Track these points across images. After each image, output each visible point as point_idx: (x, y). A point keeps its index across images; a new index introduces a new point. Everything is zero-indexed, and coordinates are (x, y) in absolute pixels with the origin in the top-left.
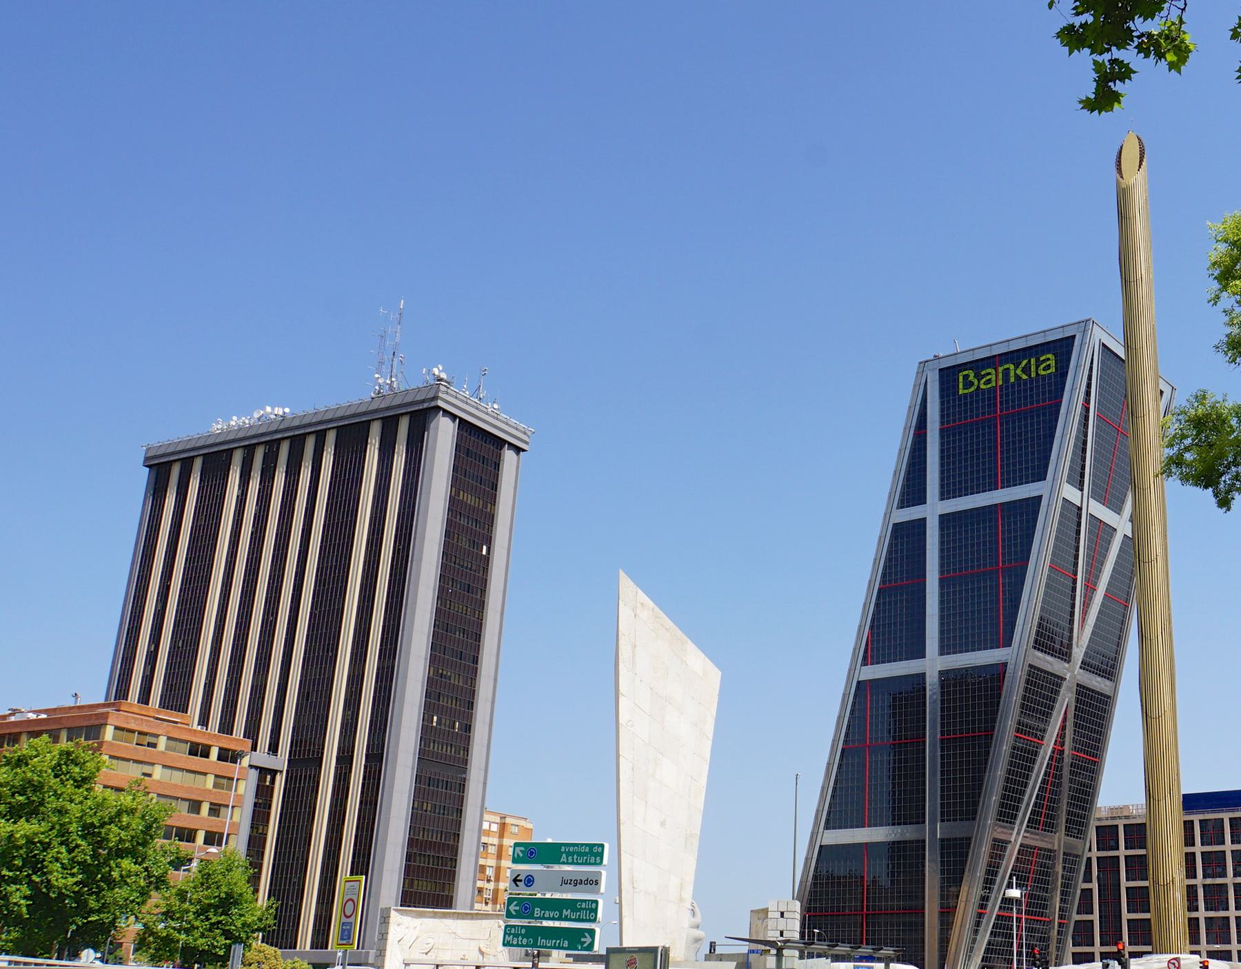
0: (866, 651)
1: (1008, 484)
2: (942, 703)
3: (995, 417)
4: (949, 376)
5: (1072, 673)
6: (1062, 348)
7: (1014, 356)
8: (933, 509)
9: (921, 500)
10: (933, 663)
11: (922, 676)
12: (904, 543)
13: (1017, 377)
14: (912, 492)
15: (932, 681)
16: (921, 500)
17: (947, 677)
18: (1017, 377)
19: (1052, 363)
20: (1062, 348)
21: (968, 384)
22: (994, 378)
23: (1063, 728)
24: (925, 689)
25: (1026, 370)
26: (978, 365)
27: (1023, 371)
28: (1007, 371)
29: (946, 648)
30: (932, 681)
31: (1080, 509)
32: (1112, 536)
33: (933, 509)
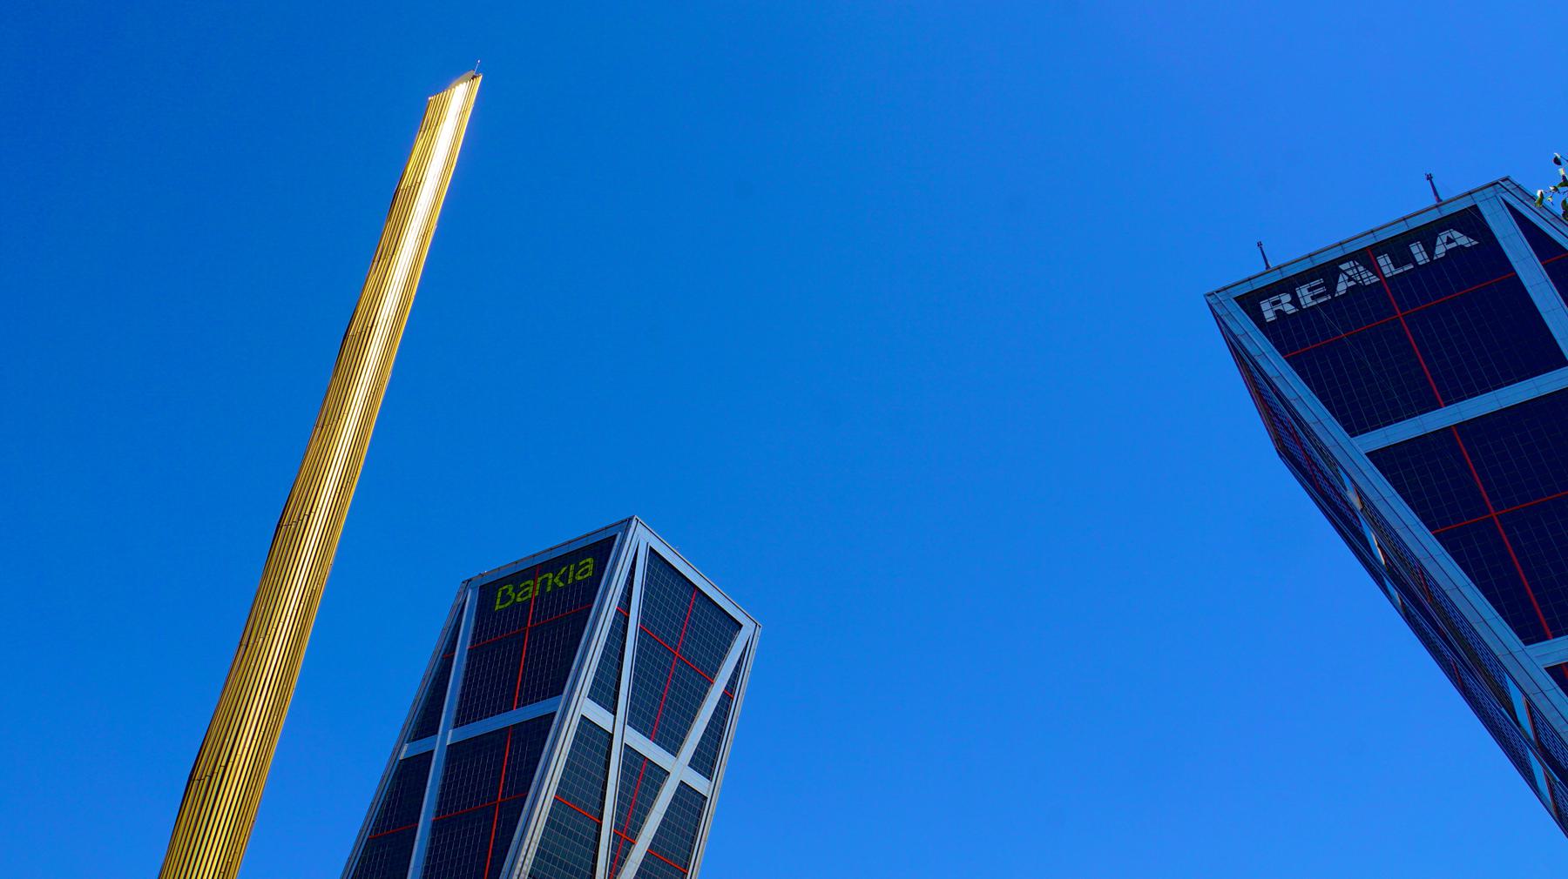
1: (524, 702)
3: (522, 632)
4: (487, 592)
6: (601, 550)
7: (553, 565)
12: (406, 779)
13: (554, 585)
18: (554, 585)
19: (590, 567)
21: (505, 598)
22: (531, 588)
25: (564, 578)
26: (517, 578)
27: (564, 578)
28: (544, 582)
31: (611, 736)
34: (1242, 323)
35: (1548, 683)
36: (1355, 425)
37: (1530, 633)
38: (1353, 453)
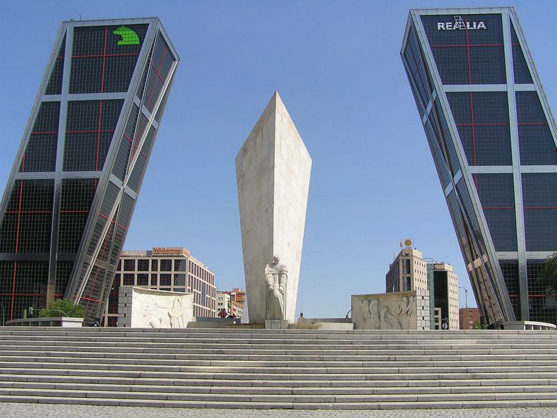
0: (22, 165)
1: (106, 91)
2: (63, 194)
5: (124, 187)
8: (65, 97)
9: (59, 92)
10: (59, 175)
11: (53, 181)
14: (54, 86)
15: (58, 184)
16: (59, 92)
17: (67, 183)
20: (141, 29)
23: (116, 212)
24: (53, 187)
29: (66, 168)
30: (58, 184)
32: (146, 123)
33: (65, 97)
34: (420, 27)
35: (471, 178)
36: (445, 82)
37: (471, 163)
38: (442, 90)
